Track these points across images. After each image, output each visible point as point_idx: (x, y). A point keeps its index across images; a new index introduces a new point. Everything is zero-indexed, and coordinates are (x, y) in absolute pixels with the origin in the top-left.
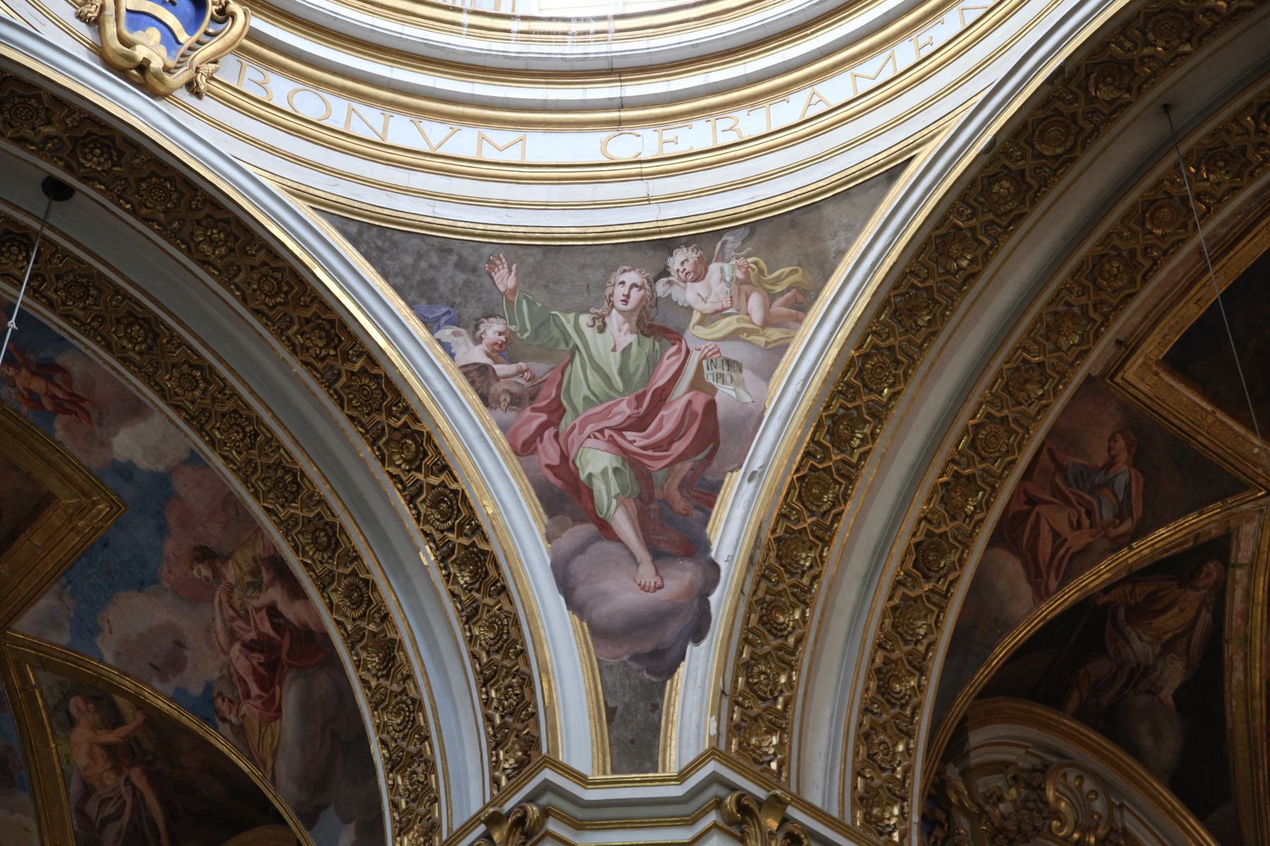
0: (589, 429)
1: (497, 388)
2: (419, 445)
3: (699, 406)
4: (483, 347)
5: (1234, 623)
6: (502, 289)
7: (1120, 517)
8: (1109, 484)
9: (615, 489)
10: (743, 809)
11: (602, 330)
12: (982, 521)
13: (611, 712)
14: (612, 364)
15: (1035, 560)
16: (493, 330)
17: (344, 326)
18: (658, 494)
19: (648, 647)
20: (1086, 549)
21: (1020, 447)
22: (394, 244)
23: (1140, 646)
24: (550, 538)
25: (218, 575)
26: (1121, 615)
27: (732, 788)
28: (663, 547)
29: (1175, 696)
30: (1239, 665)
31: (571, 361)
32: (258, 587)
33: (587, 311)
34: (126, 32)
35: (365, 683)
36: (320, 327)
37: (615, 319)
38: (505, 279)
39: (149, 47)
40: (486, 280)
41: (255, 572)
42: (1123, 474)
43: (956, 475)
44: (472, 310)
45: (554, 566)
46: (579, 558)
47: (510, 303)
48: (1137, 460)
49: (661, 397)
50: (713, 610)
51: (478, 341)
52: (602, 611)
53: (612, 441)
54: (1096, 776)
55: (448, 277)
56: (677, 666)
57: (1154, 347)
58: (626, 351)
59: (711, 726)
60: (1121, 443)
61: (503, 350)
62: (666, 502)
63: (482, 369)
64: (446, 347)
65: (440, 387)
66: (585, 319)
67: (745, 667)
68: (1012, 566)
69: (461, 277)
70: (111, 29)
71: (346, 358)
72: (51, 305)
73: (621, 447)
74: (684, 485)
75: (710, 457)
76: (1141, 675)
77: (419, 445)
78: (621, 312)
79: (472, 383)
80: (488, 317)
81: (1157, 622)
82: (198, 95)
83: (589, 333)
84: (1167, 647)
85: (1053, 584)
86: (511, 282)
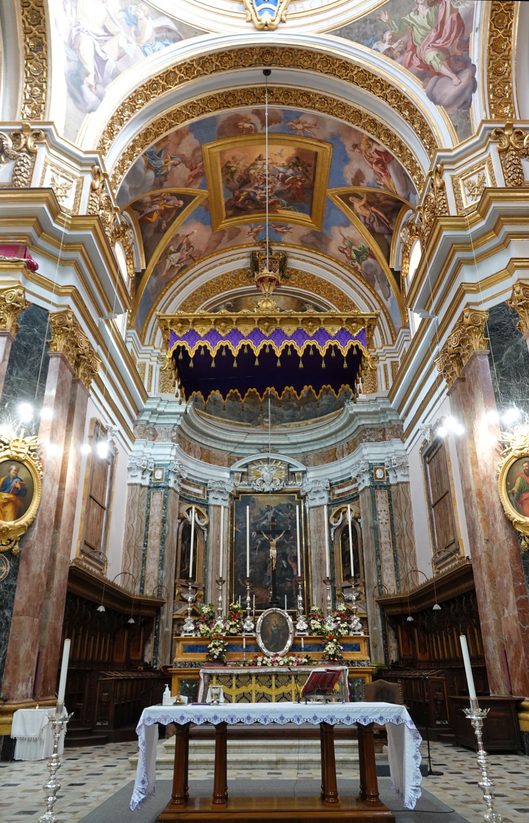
0: (425, 47)
1: (395, 52)
2: (380, 83)
3: (455, 19)
4: (387, 43)
6: (385, 21)
9: (439, 61)
11: (418, 14)
13: (456, 127)
14: (424, 22)
16: (387, 36)
17: (347, 62)
18: (452, 54)
19: (462, 102)
22: (351, 29)
24: (424, 88)
25: (360, 150)
27: (492, 129)
28: (458, 70)
31: (413, 30)
32: (370, 147)
33: (411, 11)
34: (259, 18)
35: (398, 156)
36: (342, 67)
37: (421, 8)
38: (385, 18)
39: (266, 18)
40: (380, 22)
41: (368, 144)
44: (380, 33)
45: (428, 95)
46: (435, 88)
47: (389, 24)
49: (443, 23)
50: (477, 79)
51: (384, 42)
52: (446, 100)
53: (433, 46)
55: (369, 28)
56: (471, 102)
58: (428, 16)
61: (393, 40)
62: (455, 55)
63: (389, 50)
64: (377, 50)
65: (378, 63)
66: (412, 14)
69: (372, 26)
70: (255, 19)
71: (352, 71)
72: (283, 104)
73: (436, 47)
74: (459, 46)
75: (463, 32)
77: (380, 83)
78: (422, 4)
79: (387, 56)
80: (384, 33)
82: (284, 22)
83: (414, 17)
86: (387, 17)
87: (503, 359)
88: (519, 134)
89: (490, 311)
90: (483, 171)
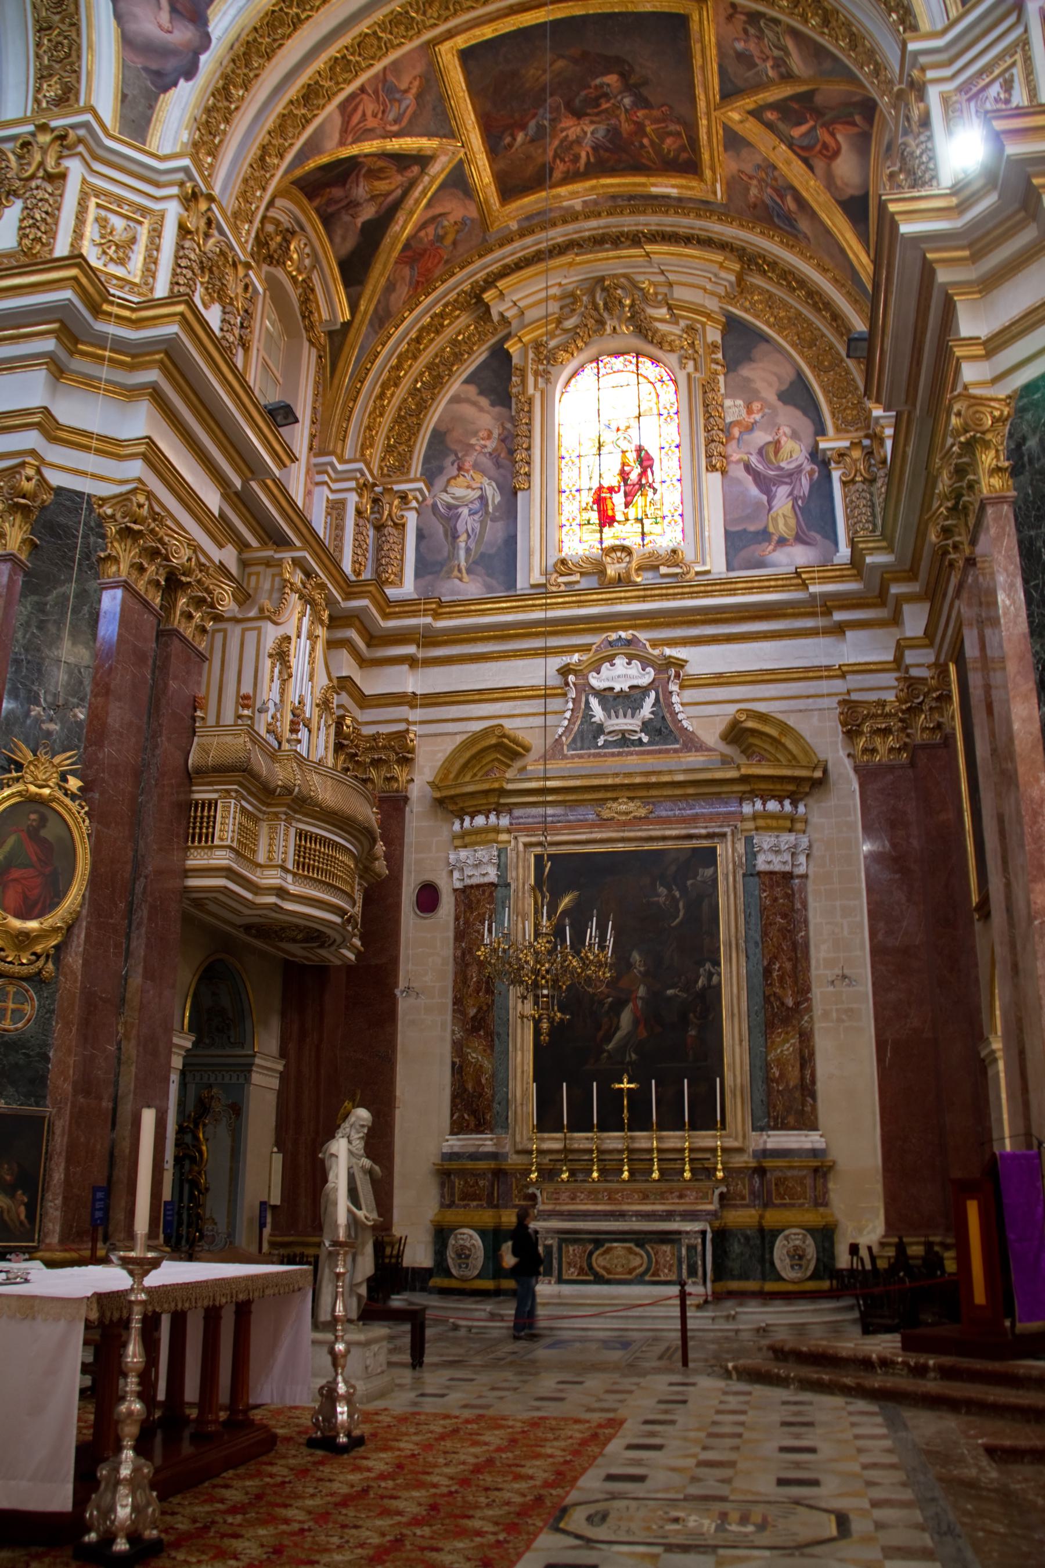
5: (410, 202)
7: (396, 121)
8: (400, 101)
10: (194, 194)
12: (342, 89)
15: (348, 122)
20: (372, 130)
21: (380, 59)
23: (361, 190)
26: (363, 171)
29: (364, 224)
30: (401, 222)
42: (410, 99)
43: (344, 57)
48: (419, 96)
54: (313, 249)
57: (461, 42)
59: (185, 137)
60: (416, 83)
67: (208, 111)
68: (338, 120)
76: (353, 205)
81: (377, 183)
84: (373, 198)
85: (350, 140)
87: (50, 598)
88: (209, 223)
89: (59, 491)
90: (138, 228)
